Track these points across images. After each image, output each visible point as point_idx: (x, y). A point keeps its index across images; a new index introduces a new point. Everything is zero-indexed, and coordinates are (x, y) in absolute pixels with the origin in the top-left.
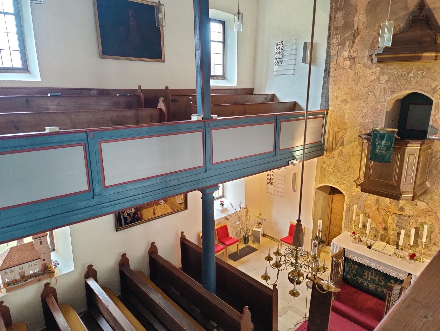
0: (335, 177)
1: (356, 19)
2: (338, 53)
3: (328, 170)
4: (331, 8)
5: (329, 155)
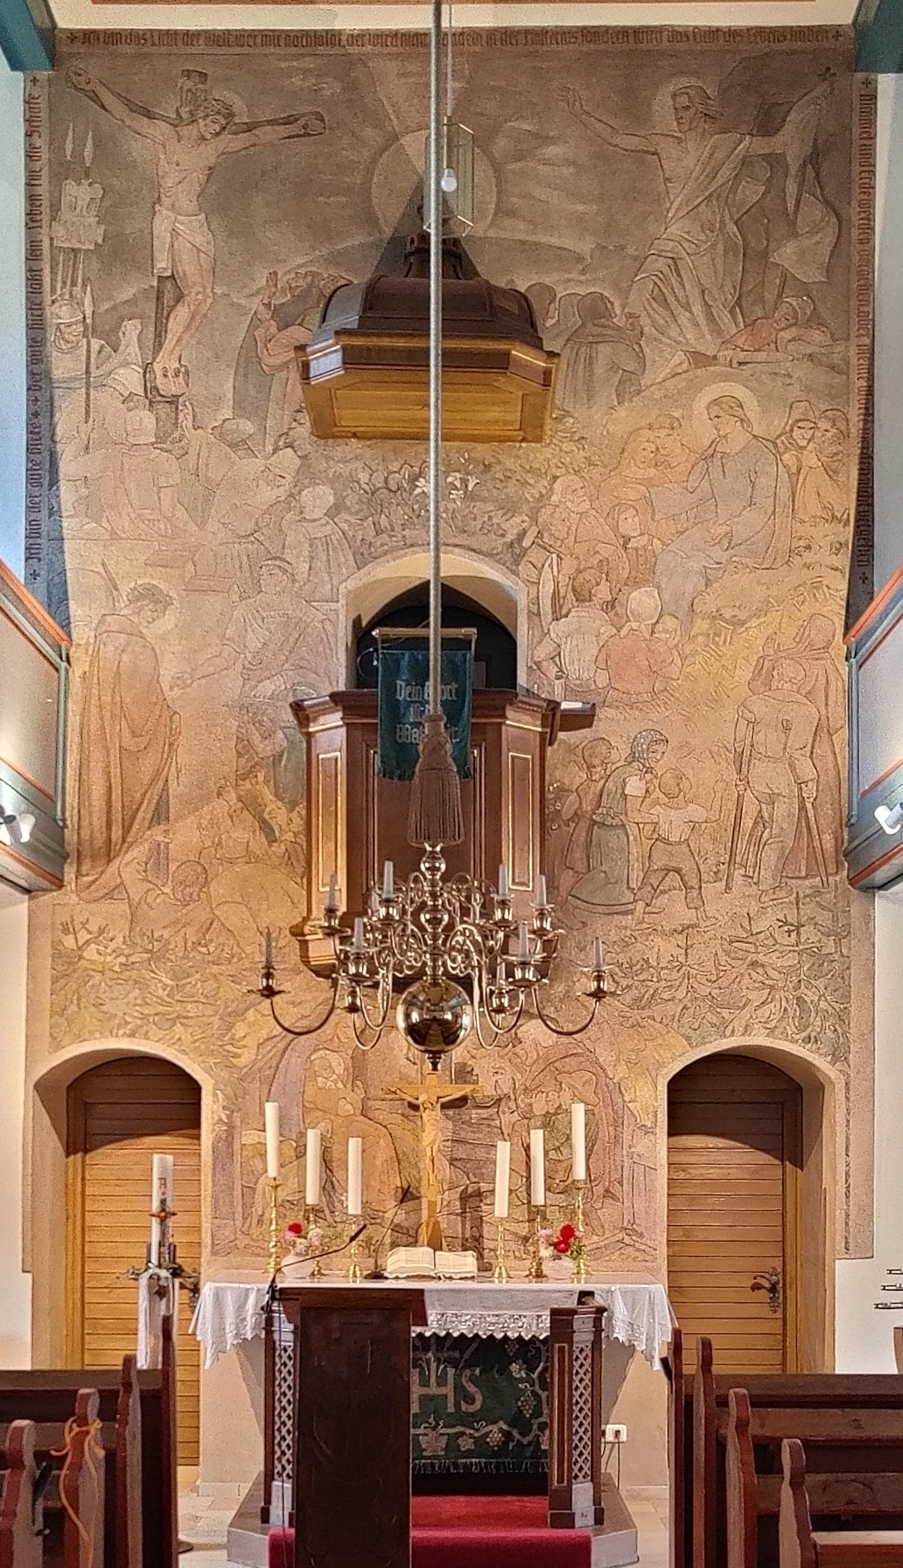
0: (137, 991)
1: (161, 226)
2: (88, 372)
3: (92, 962)
4: (31, 155)
5: (94, 882)
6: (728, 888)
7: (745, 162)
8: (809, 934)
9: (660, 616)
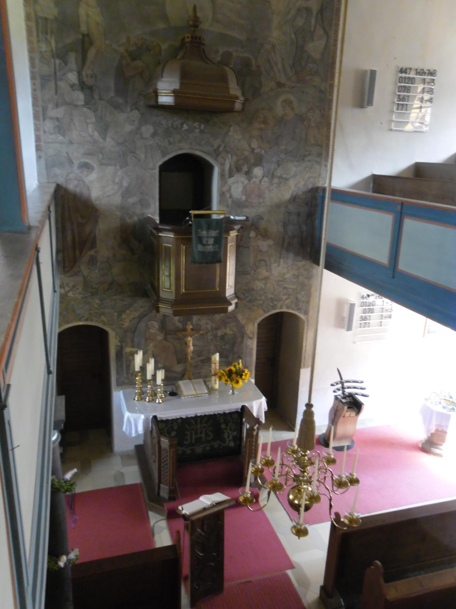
2: (55, 73)
6: (279, 266)
7: (299, 10)
8: (301, 279)
9: (263, 177)
